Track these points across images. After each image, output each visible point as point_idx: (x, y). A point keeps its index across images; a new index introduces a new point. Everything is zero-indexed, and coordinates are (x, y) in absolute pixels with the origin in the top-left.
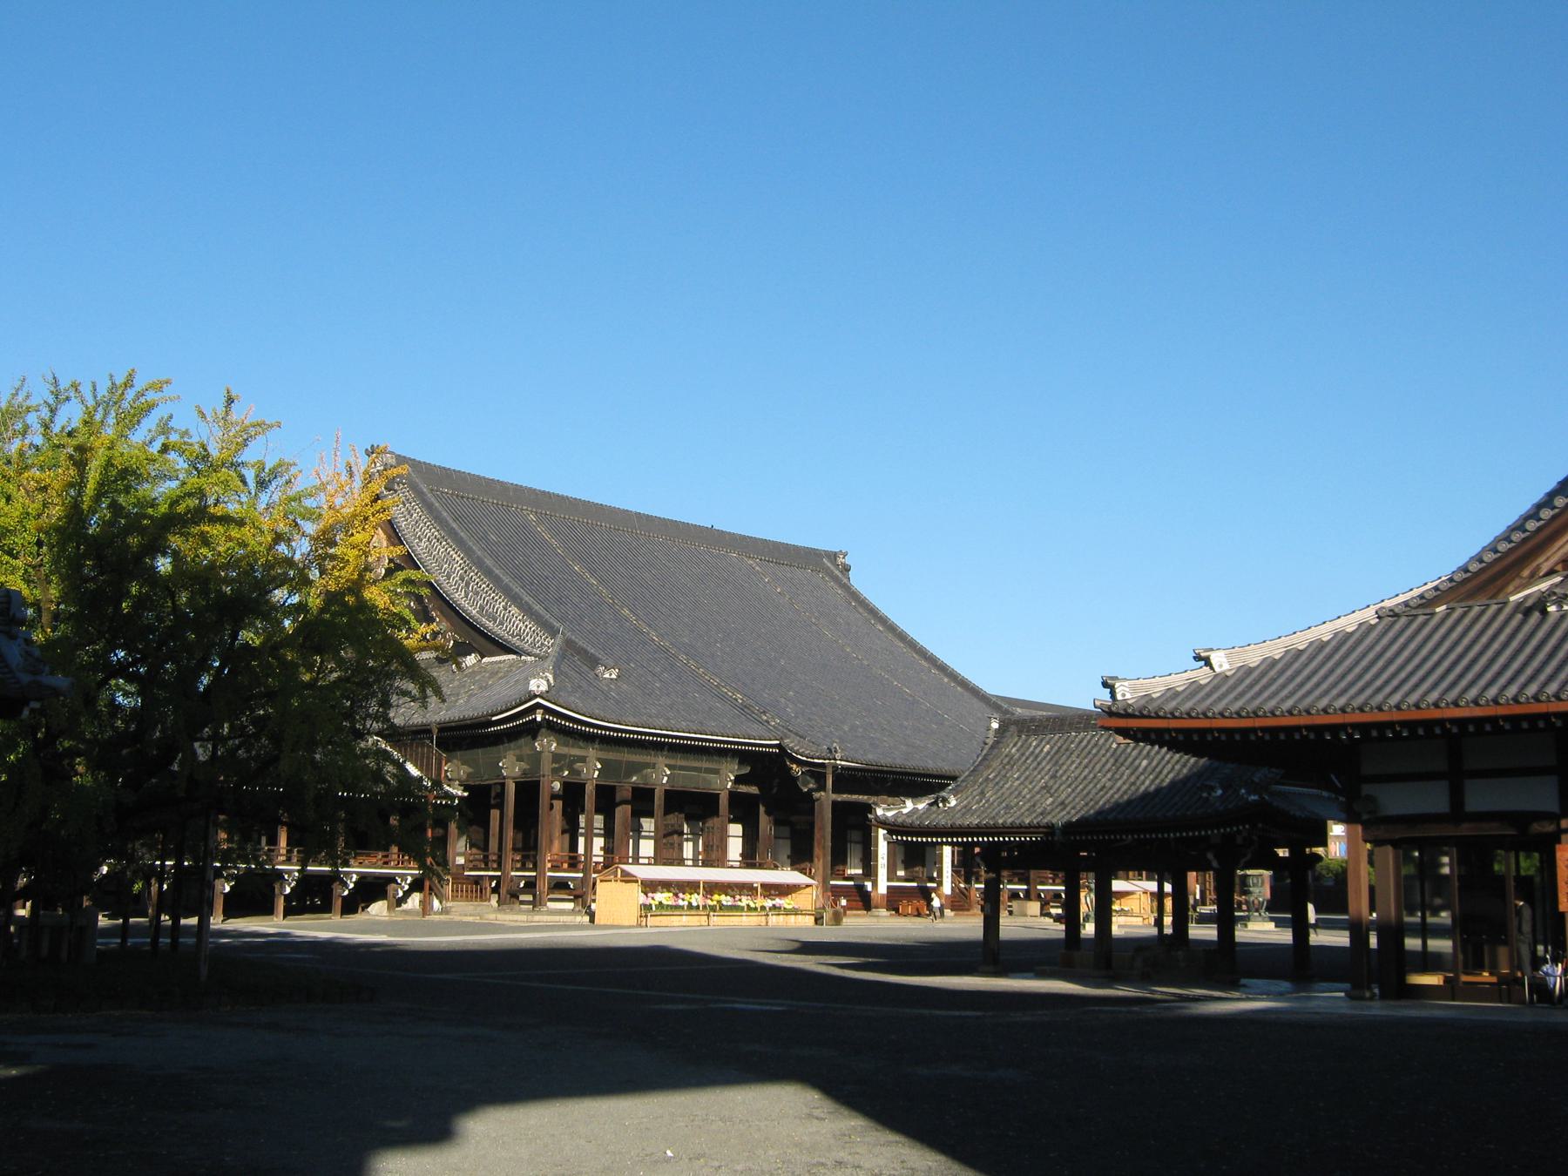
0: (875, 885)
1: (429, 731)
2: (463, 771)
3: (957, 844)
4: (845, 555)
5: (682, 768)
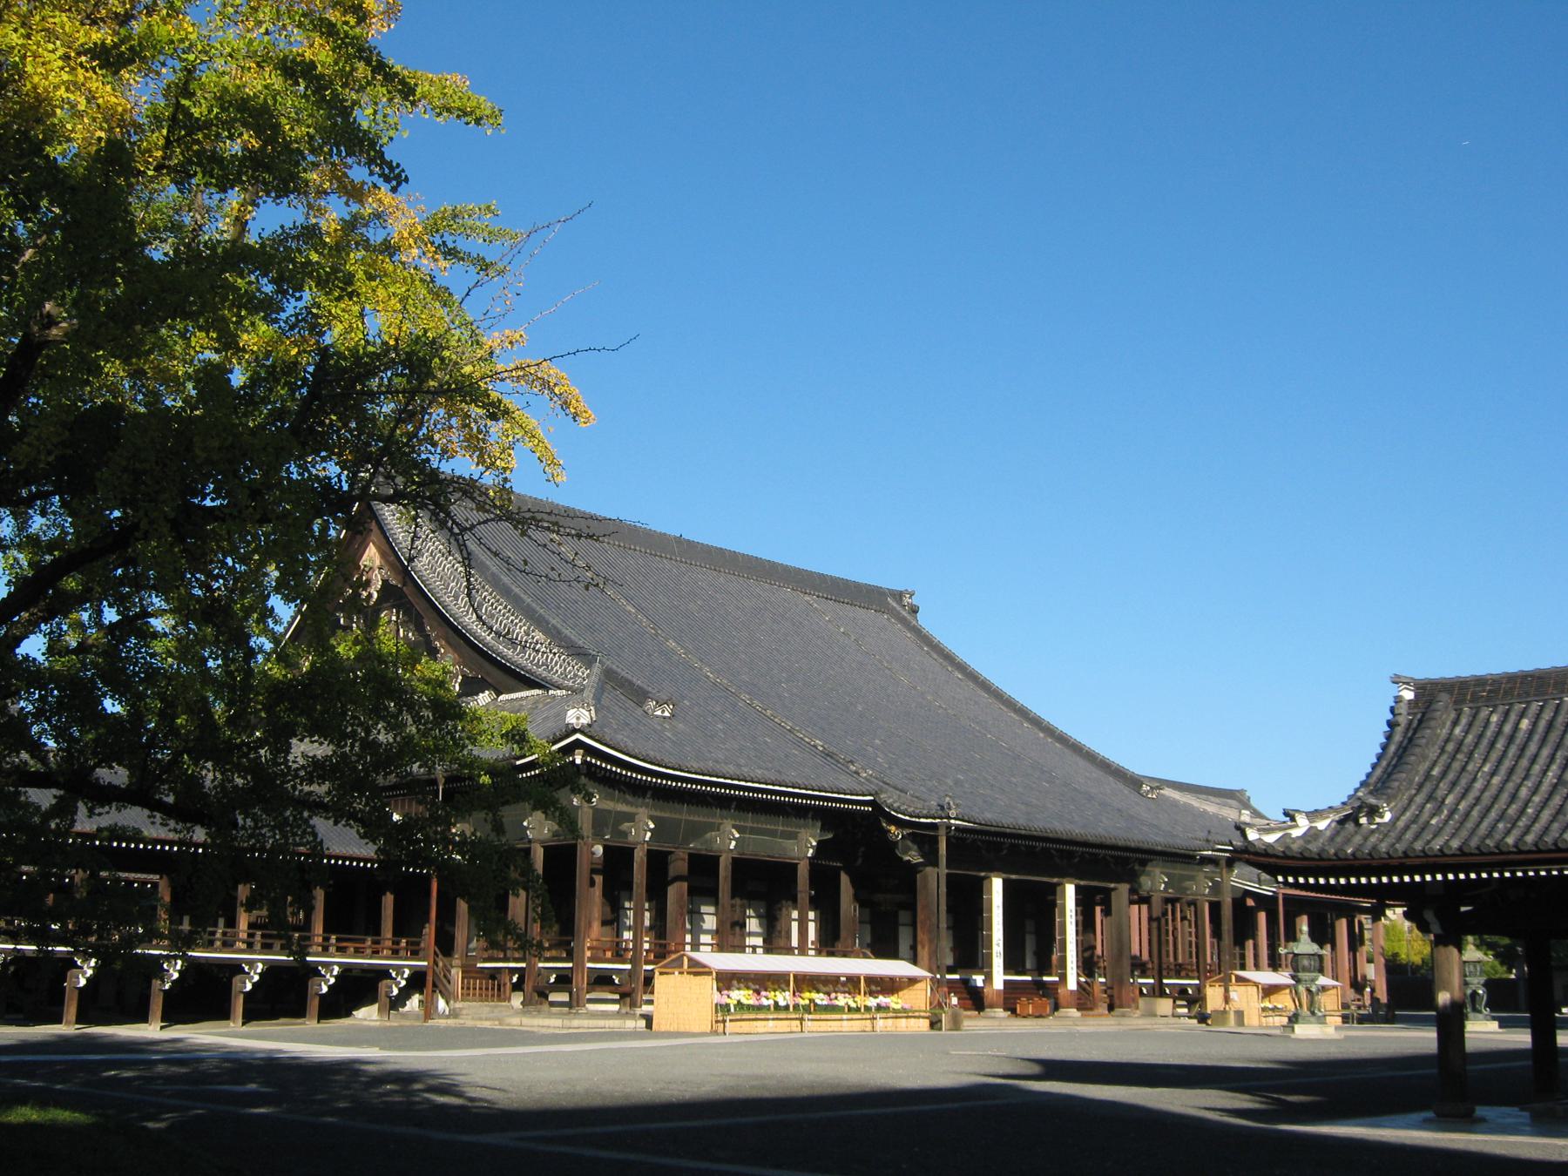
0: (989, 978)
5: (753, 831)
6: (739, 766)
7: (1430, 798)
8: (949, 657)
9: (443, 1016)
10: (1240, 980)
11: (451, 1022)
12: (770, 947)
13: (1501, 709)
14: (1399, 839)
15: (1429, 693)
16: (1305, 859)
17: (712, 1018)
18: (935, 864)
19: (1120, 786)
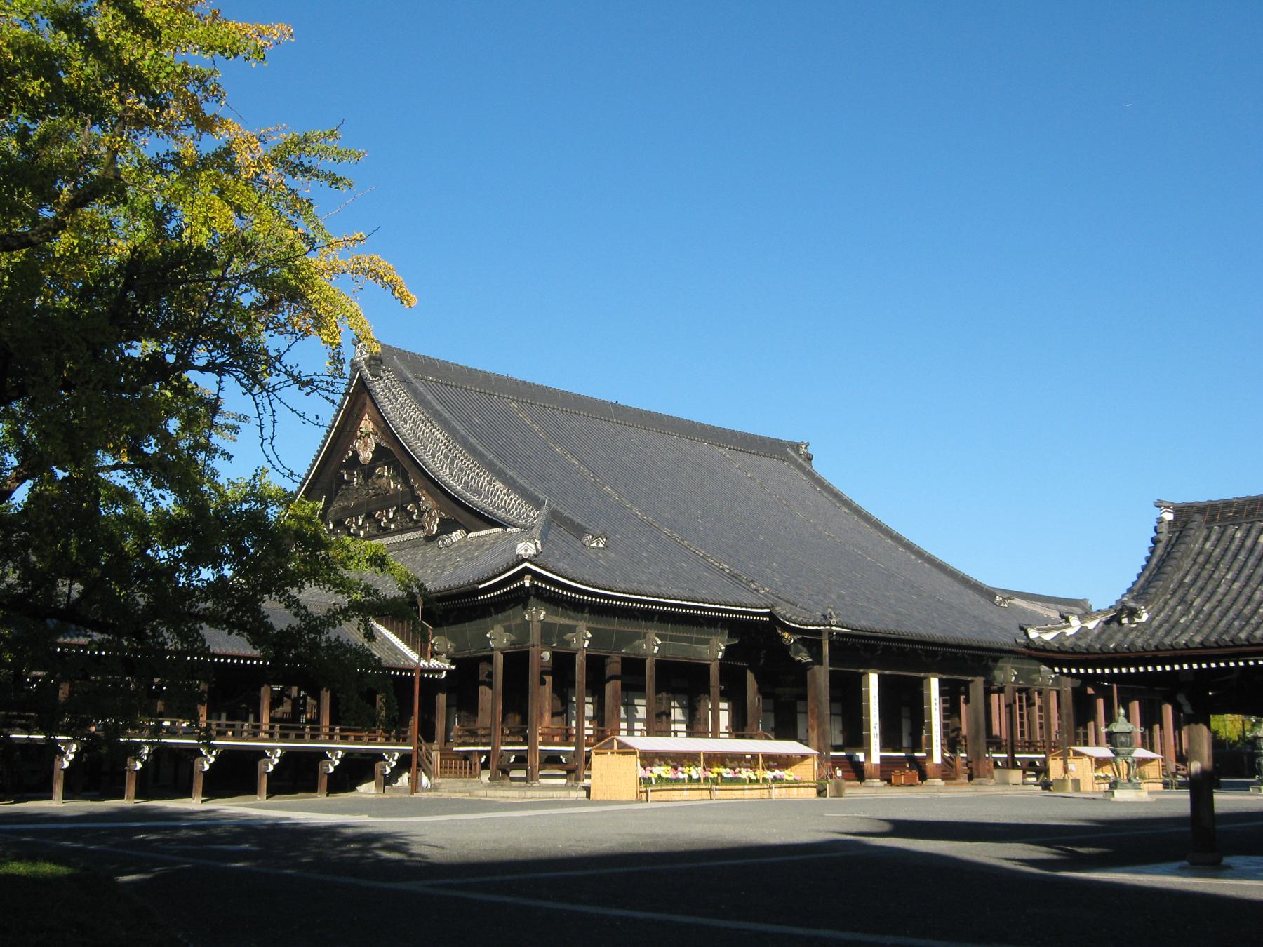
0: (868, 755)
5: (672, 638)
6: (659, 586)
7: (1182, 601)
8: (837, 496)
9: (426, 790)
10: (1077, 754)
11: (432, 794)
12: (691, 732)
13: (1244, 526)
14: (1153, 636)
15: (1185, 514)
16: (1075, 653)
17: (637, 789)
18: (821, 663)
19: (977, 597)
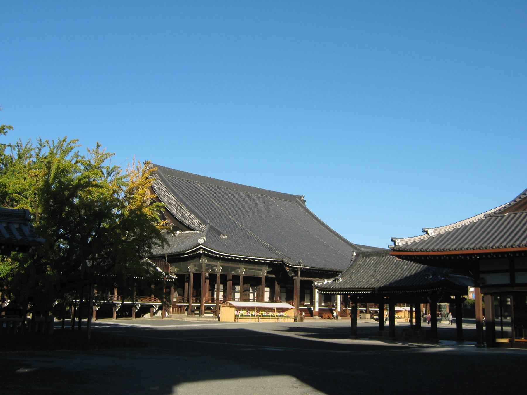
1: (165, 257)
2: (176, 270)
3: (342, 294)
4: (304, 197)
11: (169, 319)
